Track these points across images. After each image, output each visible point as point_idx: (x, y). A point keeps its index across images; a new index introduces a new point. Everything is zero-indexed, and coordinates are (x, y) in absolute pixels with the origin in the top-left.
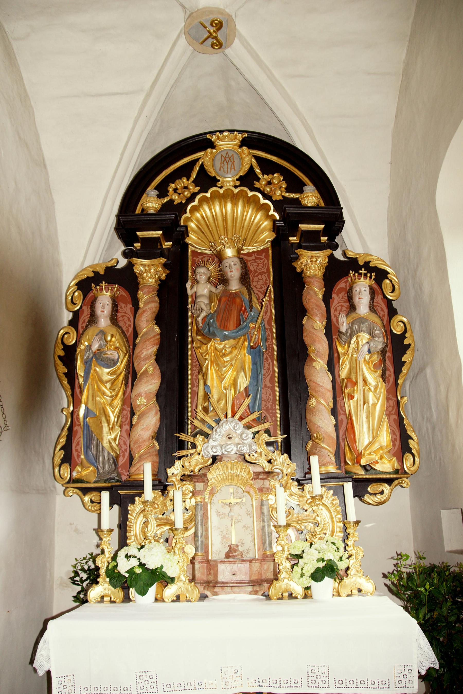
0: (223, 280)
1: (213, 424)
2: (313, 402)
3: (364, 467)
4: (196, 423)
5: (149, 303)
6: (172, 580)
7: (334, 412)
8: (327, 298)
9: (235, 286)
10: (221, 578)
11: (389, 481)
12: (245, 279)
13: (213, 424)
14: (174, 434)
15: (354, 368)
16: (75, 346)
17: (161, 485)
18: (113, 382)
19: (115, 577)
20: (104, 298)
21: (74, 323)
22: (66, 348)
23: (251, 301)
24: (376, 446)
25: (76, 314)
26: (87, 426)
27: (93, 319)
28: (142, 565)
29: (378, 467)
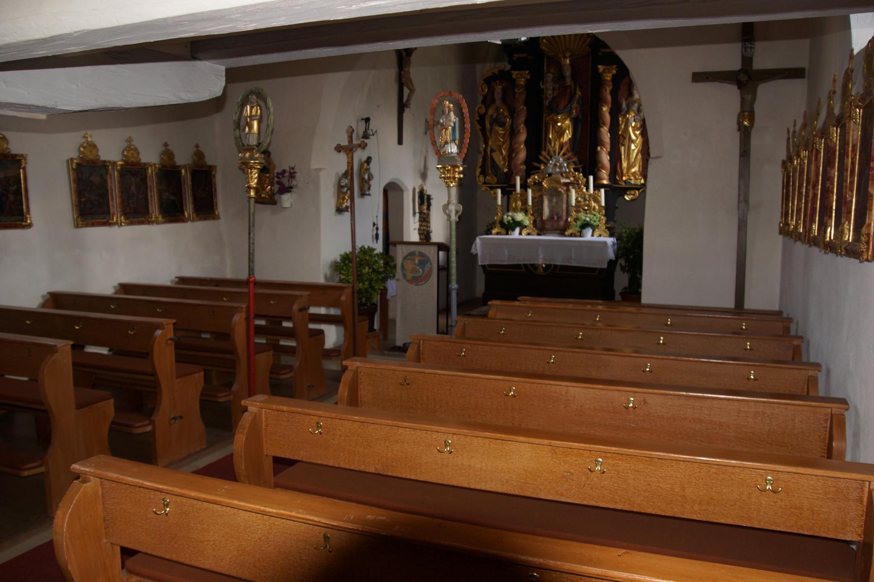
0: (561, 77)
1: (548, 158)
2: (599, 148)
3: (625, 181)
4: (541, 158)
5: (521, 95)
6: (526, 227)
7: (610, 154)
8: (614, 93)
9: (569, 81)
10: (547, 227)
11: (638, 189)
12: (573, 76)
13: (548, 158)
14: (533, 163)
15: (626, 130)
16: (485, 114)
17: (524, 186)
18: (504, 135)
19: (502, 224)
20: (498, 88)
21: (483, 102)
22: (480, 116)
23: (575, 90)
24: (633, 170)
25: (485, 96)
26: (492, 157)
27: (493, 101)
28: (513, 219)
29: (632, 182)
